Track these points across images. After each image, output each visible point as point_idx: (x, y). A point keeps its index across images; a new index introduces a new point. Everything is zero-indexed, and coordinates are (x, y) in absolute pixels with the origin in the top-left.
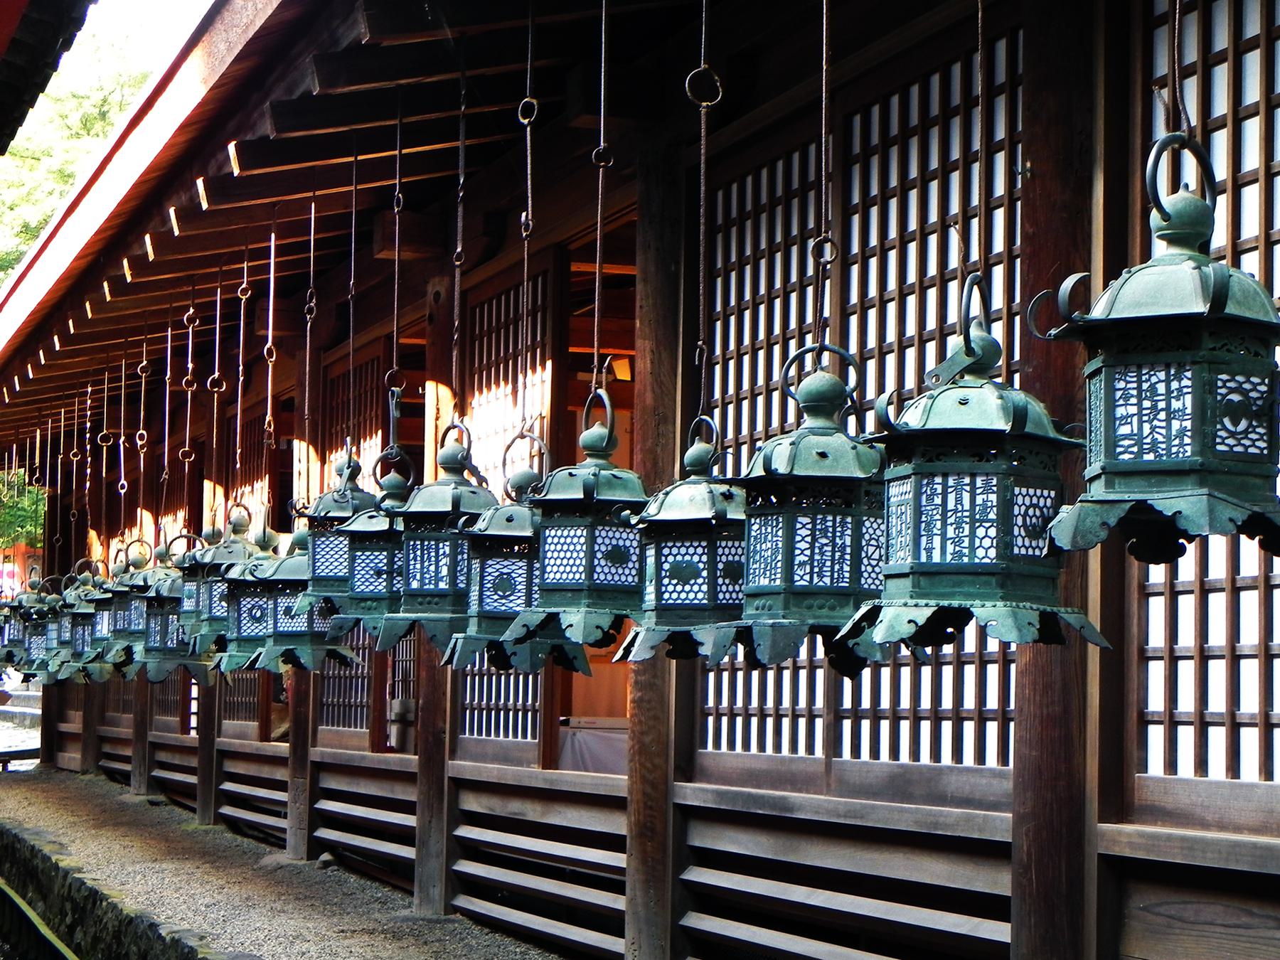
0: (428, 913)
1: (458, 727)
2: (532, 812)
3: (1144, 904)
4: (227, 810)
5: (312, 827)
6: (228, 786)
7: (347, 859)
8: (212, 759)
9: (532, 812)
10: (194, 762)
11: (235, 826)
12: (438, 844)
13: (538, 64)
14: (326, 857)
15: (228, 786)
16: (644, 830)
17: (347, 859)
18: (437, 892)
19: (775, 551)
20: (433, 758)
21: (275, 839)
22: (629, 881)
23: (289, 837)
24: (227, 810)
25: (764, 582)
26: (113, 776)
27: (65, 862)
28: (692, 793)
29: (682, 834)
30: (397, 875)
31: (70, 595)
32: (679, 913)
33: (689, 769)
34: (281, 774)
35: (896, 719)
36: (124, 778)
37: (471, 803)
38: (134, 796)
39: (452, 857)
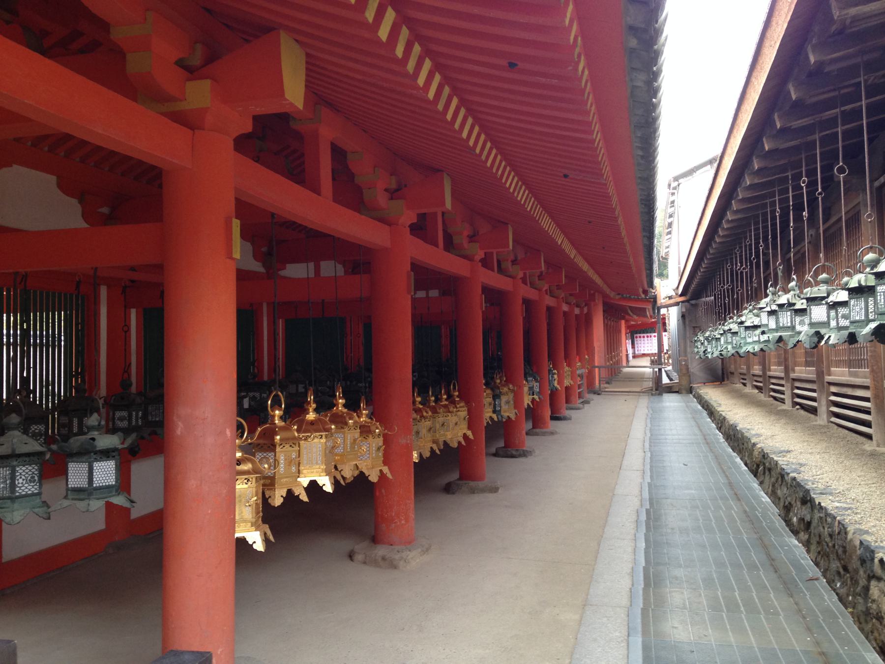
0: (821, 423)
2: (849, 391)
4: (772, 394)
5: (793, 398)
6: (772, 386)
7: (803, 407)
8: (766, 377)
9: (849, 391)
11: (775, 398)
12: (824, 402)
13: (814, 166)
14: (798, 407)
15: (772, 386)
17: (803, 407)
18: (825, 416)
19: (861, 309)
20: (820, 374)
21: (782, 401)
22: (872, 411)
23: (786, 401)
25: (857, 318)
27: (719, 409)
30: (813, 411)
34: (783, 382)
37: (833, 389)
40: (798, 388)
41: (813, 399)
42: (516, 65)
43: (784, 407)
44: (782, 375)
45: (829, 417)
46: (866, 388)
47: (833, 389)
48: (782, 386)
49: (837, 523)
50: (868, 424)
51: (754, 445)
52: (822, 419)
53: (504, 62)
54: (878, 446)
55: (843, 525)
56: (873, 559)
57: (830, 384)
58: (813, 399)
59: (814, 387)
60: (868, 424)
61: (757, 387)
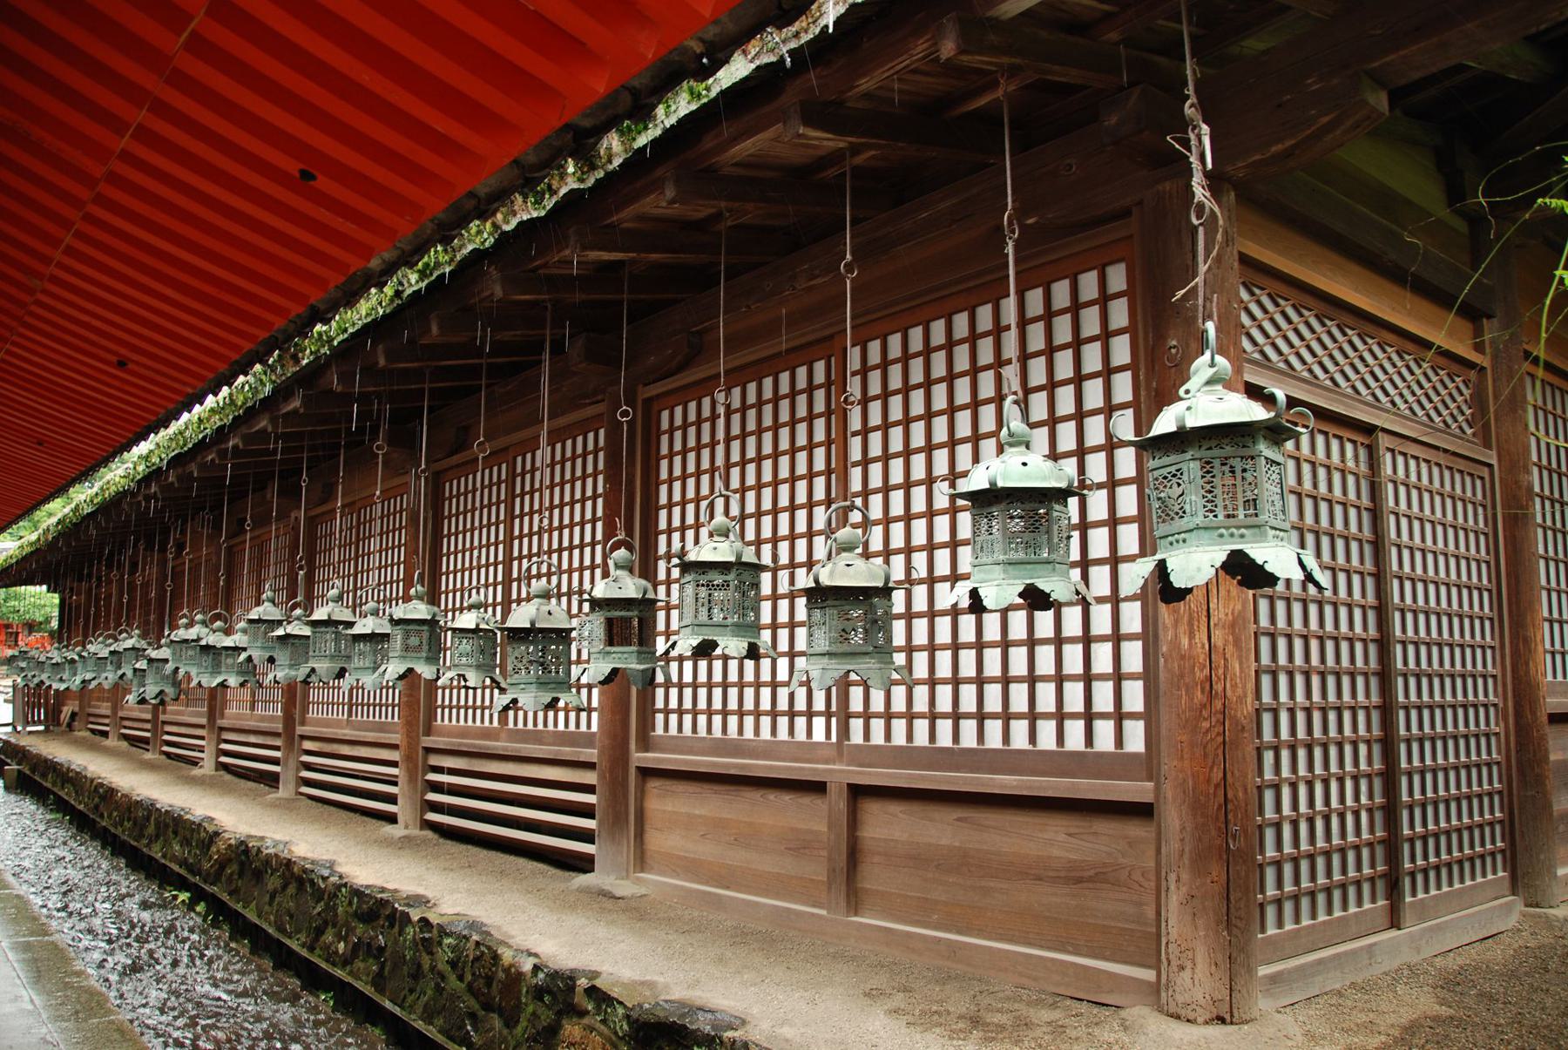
1: (305, 710)
2: (346, 750)
3: (653, 785)
4: (165, 748)
6: (166, 737)
9: (346, 750)
10: (148, 726)
11: (168, 755)
12: (292, 764)
15: (166, 737)
16: (409, 758)
18: (292, 786)
24: (165, 748)
26: (93, 731)
28: (428, 741)
29: (425, 759)
30: (272, 780)
31: (91, 648)
32: (424, 794)
33: (428, 731)
35: (451, 708)
36: (105, 734)
37: (308, 745)
38: (112, 742)
39: (298, 770)
40: (227, 742)
41: (275, 762)
42: (313, 177)
43: (196, 772)
44: (204, 721)
45: (298, 785)
46: (395, 747)
47: (308, 745)
48: (202, 738)
49: (471, 945)
50: (392, 799)
51: (217, 834)
52: (285, 791)
53: (293, 167)
54: (406, 827)
55: (489, 948)
56: (571, 988)
57: (303, 737)
58: (275, 762)
59: (278, 742)
60: (392, 799)
61: (126, 737)
